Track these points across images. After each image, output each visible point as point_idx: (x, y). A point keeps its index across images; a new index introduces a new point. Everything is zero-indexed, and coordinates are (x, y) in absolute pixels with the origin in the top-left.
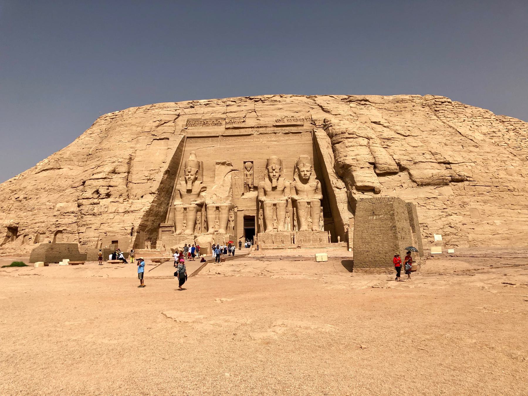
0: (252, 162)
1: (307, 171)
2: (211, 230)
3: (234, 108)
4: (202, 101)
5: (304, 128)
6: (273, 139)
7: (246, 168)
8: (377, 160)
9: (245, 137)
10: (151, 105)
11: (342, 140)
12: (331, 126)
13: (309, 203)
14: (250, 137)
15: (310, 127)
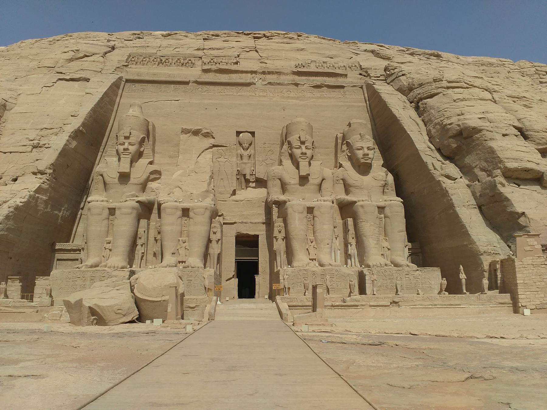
0: (253, 133)
1: (368, 148)
2: (169, 259)
3: (217, 43)
4: (159, 33)
5: (348, 80)
6: (292, 95)
7: (240, 144)
8: (527, 124)
9: (240, 87)
10: (63, 36)
11: (439, 90)
12: (403, 75)
13: (381, 209)
14: (249, 88)
15: (358, 78)
